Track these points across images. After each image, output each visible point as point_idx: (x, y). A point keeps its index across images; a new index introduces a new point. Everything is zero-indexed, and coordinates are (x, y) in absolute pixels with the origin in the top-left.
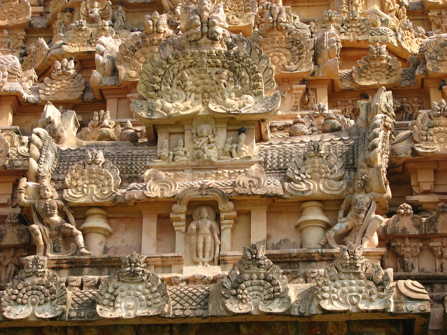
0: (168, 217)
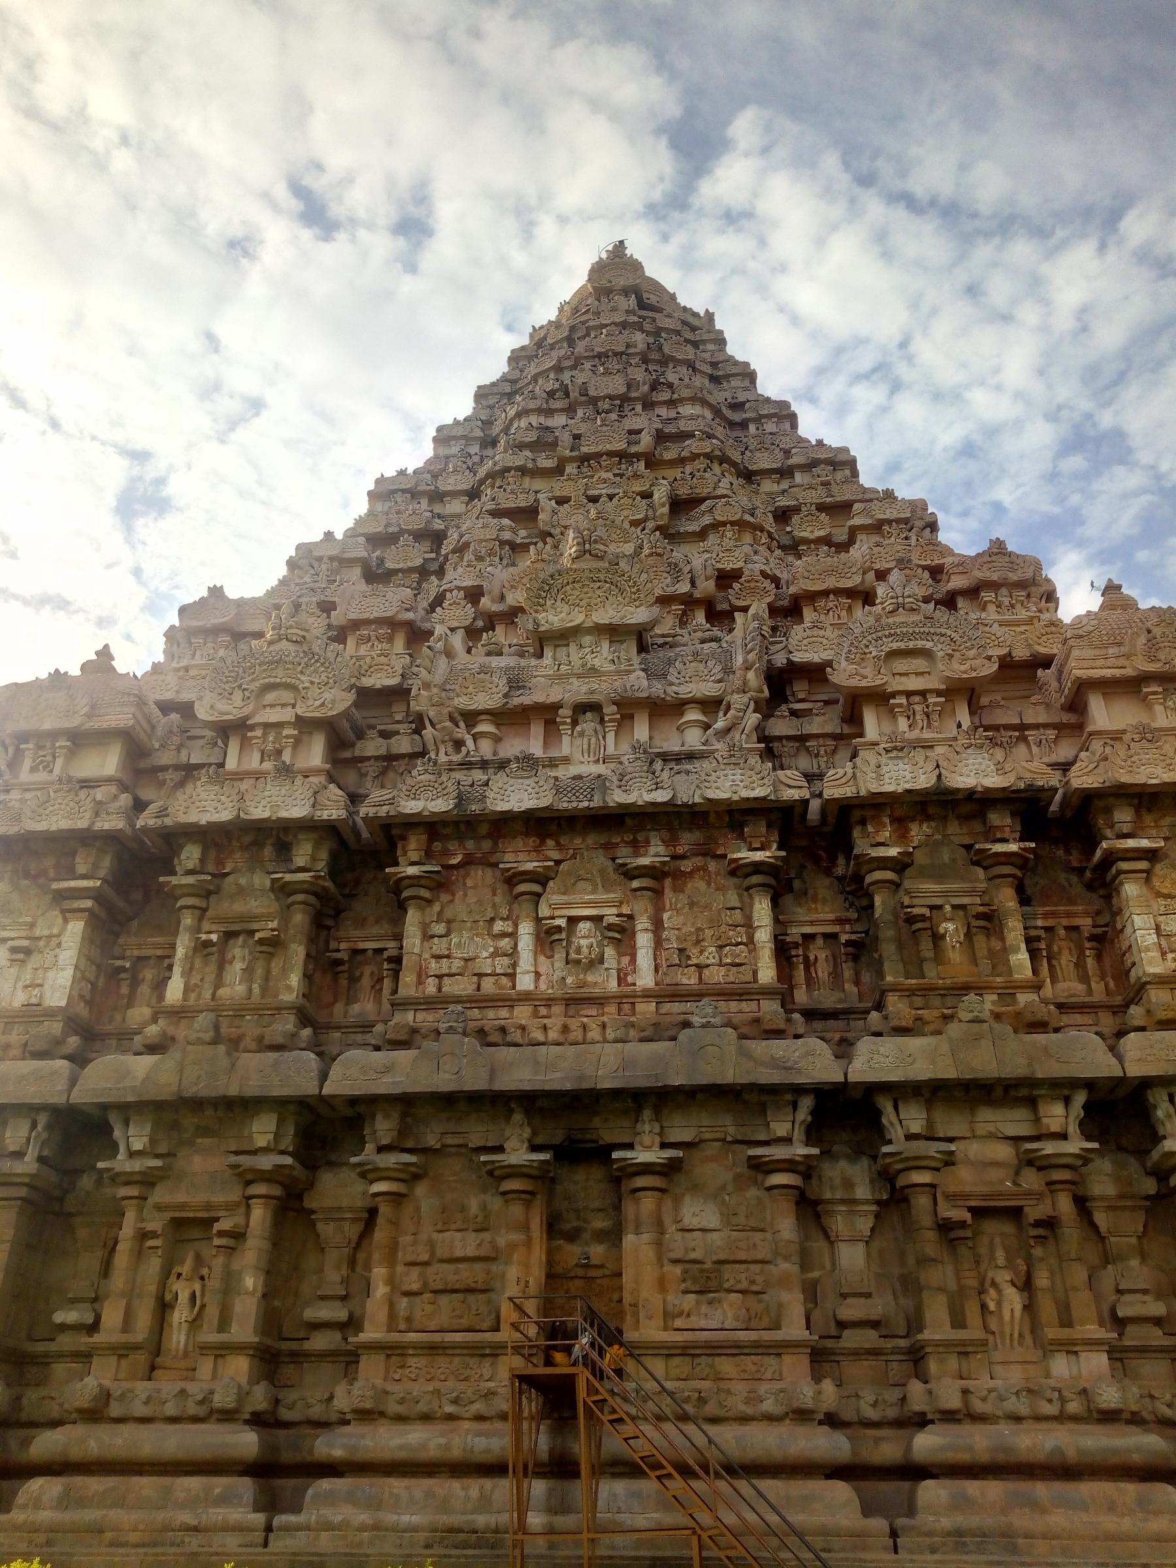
0: (555, 722)
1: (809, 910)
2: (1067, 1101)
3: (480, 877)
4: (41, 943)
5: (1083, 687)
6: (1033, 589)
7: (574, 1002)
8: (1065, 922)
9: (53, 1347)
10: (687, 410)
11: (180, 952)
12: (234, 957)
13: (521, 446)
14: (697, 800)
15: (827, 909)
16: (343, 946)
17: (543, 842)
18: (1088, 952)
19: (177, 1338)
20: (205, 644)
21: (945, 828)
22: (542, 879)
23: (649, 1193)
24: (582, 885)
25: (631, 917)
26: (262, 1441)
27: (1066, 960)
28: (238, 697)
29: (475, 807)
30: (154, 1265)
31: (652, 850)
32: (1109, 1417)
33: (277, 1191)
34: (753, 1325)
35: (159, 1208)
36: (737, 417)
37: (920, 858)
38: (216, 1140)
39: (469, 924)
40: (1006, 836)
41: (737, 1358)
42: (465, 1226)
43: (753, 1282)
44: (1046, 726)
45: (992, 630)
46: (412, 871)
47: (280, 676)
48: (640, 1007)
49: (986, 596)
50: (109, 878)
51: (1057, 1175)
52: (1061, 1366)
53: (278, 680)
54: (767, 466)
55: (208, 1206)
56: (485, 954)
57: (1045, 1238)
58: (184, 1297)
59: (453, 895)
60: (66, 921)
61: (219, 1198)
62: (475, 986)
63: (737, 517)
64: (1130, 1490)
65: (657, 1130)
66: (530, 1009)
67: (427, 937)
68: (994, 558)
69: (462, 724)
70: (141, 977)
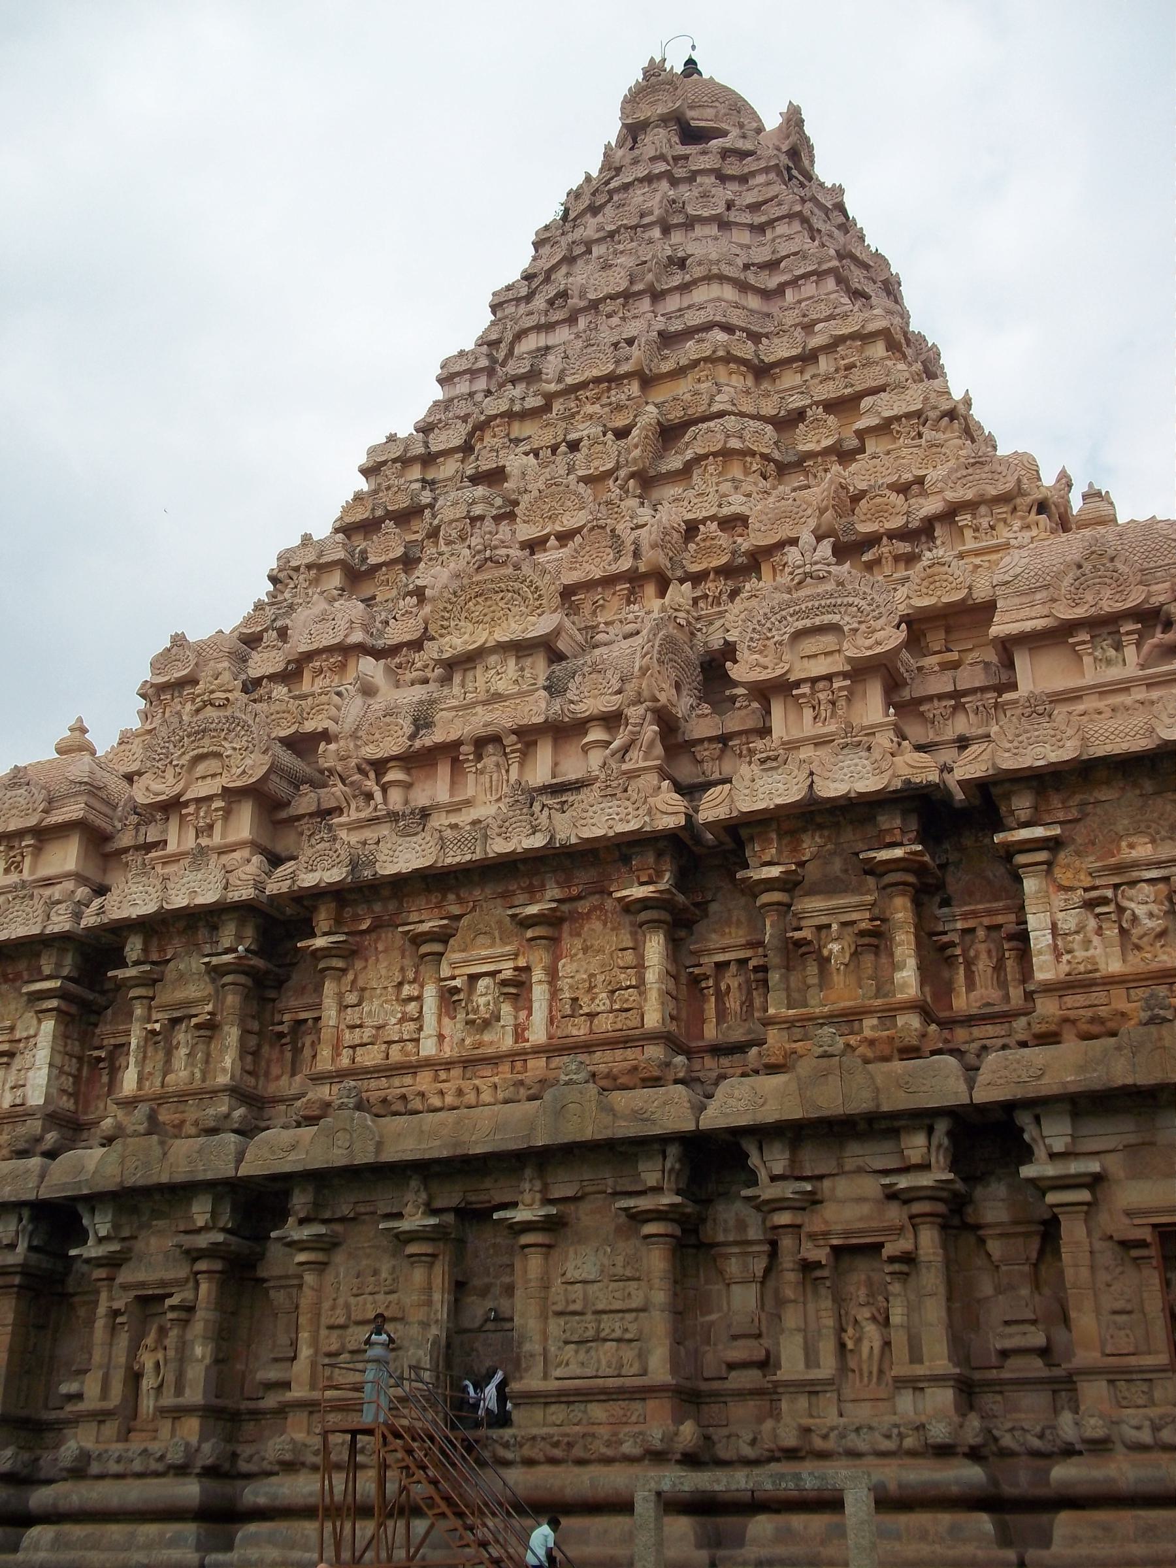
1: (723, 935)
2: (930, 1131)
3: (394, 938)
4: (22, 1045)
5: (1008, 647)
6: (1019, 501)
7: (469, 1063)
8: (986, 921)
9: (62, 1415)
10: (700, 294)
11: (134, 1042)
12: (179, 1043)
13: (514, 380)
14: (574, 840)
15: (741, 933)
16: (286, 1017)
17: (444, 898)
18: (1007, 954)
19: (147, 1404)
20: (173, 699)
21: (795, 850)
22: (443, 937)
23: (532, 1249)
24: (481, 940)
25: (528, 969)
26: (203, 1491)
27: (984, 965)
28: (170, 772)
29: (367, 873)
30: (123, 1341)
31: (549, 894)
32: (943, 1451)
33: (218, 1266)
34: (624, 1372)
35: (125, 1287)
36: (773, 282)
37: (812, 872)
38: (168, 1221)
39: (378, 991)
40: (899, 839)
41: (606, 1405)
42: (376, 1289)
43: (626, 1330)
44: (983, 689)
45: (950, 571)
46: (320, 942)
47: (207, 746)
48: (530, 1064)
49: (964, 519)
50: (75, 974)
51: (918, 1208)
52: (906, 1402)
53: (205, 750)
54: (786, 354)
55: (163, 1284)
56: (393, 1021)
57: (907, 1274)
58: (149, 1366)
59: (366, 960)
60: (40, 1021)
61: (169, 1275)
62: (383, 1055)
63: (719, 446)
64: (946, 1519)
65: (538, 1185)
66: (432, 1074)
67: (343, 1007)
68: (970, 471)
69: (372, 775)
70: (117, 1065)
